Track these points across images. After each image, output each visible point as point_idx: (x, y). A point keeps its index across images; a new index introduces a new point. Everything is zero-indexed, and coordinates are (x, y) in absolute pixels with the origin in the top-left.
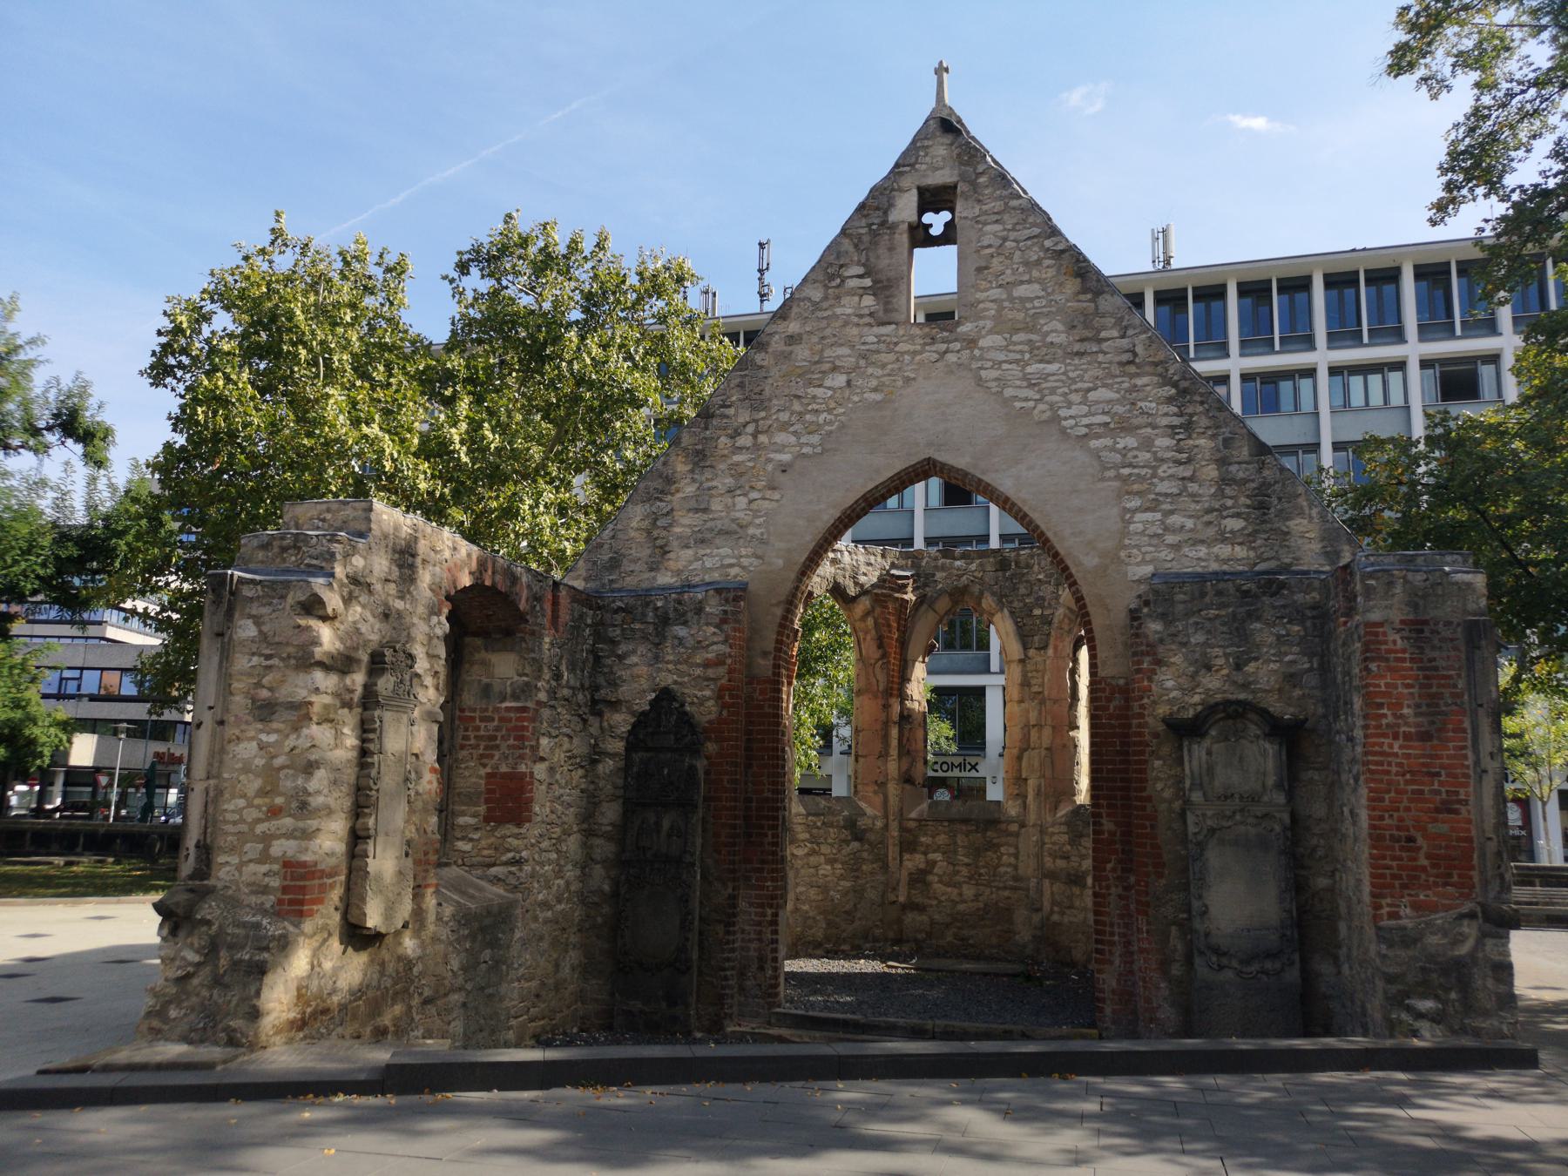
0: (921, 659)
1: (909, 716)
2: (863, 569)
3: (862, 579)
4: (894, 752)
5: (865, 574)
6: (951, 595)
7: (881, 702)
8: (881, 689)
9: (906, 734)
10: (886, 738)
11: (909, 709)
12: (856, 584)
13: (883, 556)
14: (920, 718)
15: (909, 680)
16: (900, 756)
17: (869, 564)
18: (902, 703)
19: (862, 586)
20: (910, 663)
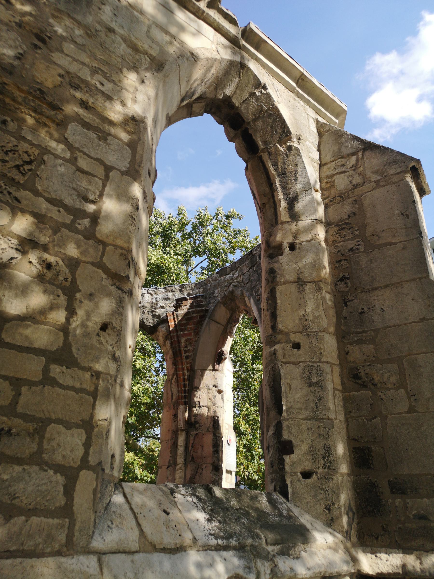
0: (211, 367)
1: (196, 422)
2: (161, 303)
3: (159, 311)
4: (180, 460)
5: (162, 307)
6: (224, 304)
7: (172, 412)
8: (173, 400)
9: (191, 441)
10: (175, 445)
11: (196, 415)
12: (154, 316)
13: (181, 291)
14: (209, 423)
15: (197, 388)
16: (186, 464)
17: (167, 299)
18: (190, 411)
19: (159, 316)
20: (199, 373)
